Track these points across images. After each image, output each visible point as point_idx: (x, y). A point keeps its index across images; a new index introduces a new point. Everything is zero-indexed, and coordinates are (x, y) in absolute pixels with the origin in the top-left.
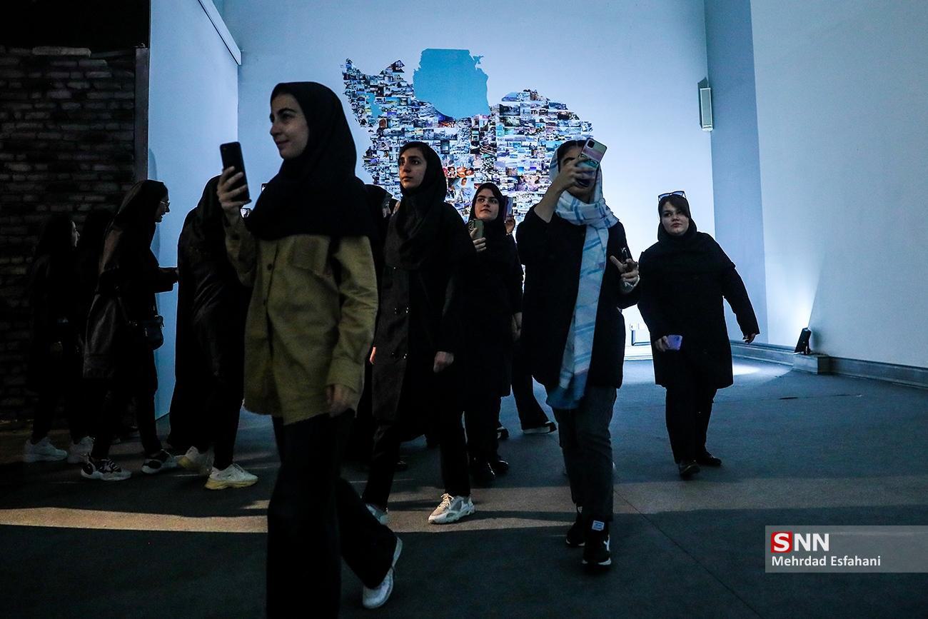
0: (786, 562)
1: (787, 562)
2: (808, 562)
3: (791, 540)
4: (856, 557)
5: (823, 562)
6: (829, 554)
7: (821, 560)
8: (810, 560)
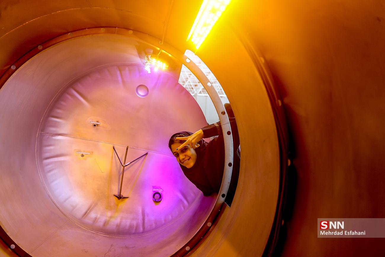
0: (326, 233)
1: (326, 233)
2: (335, 233)
3: (328, 224)
4: (355, 231)
5: (341, 233)
6: (344, 230)
7: (341, 232)
8: (336, 232)
